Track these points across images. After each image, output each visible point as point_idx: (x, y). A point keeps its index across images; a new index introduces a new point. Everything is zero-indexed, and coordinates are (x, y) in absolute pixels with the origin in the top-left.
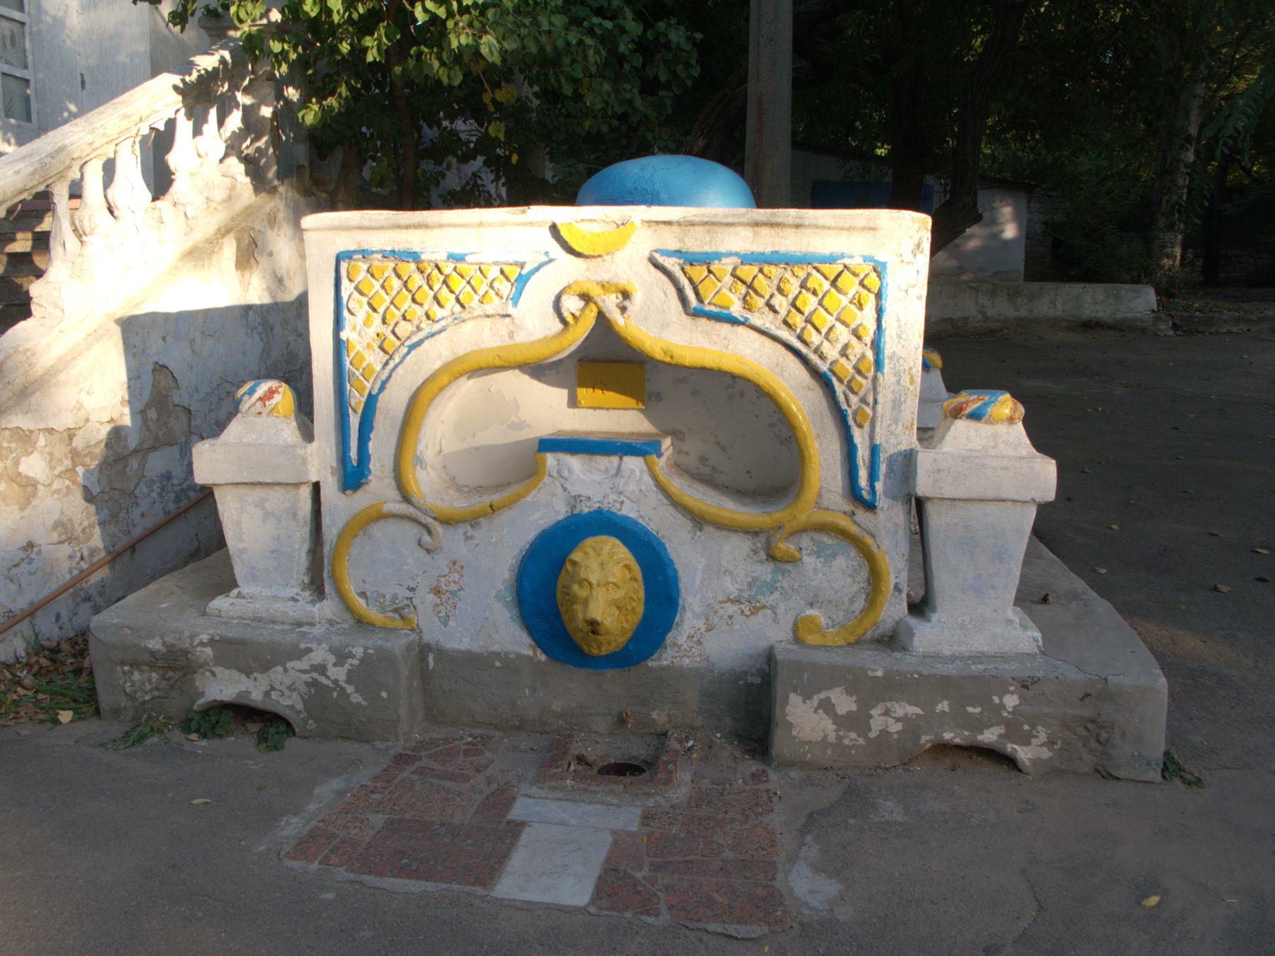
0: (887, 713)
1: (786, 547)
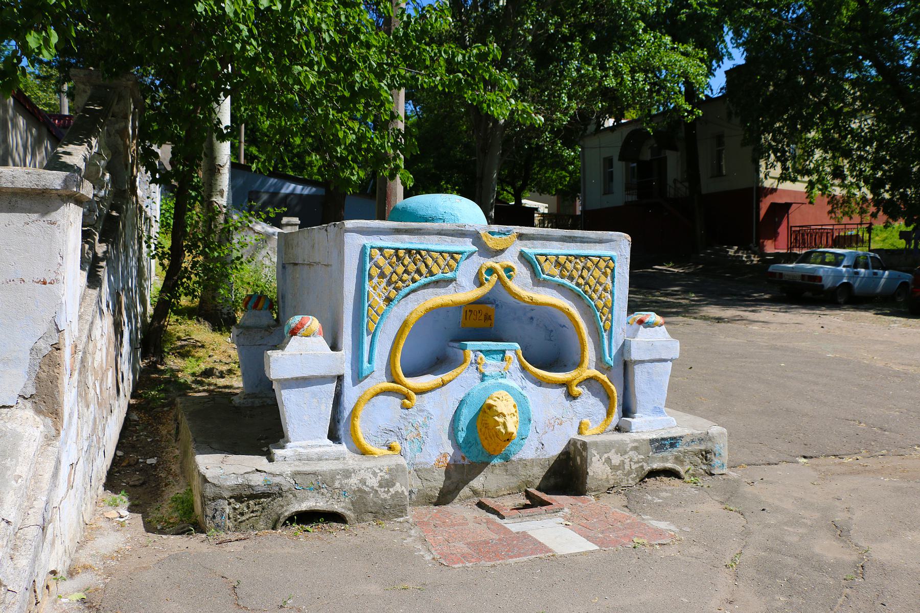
0: (631, 461)
1: (577, 390)
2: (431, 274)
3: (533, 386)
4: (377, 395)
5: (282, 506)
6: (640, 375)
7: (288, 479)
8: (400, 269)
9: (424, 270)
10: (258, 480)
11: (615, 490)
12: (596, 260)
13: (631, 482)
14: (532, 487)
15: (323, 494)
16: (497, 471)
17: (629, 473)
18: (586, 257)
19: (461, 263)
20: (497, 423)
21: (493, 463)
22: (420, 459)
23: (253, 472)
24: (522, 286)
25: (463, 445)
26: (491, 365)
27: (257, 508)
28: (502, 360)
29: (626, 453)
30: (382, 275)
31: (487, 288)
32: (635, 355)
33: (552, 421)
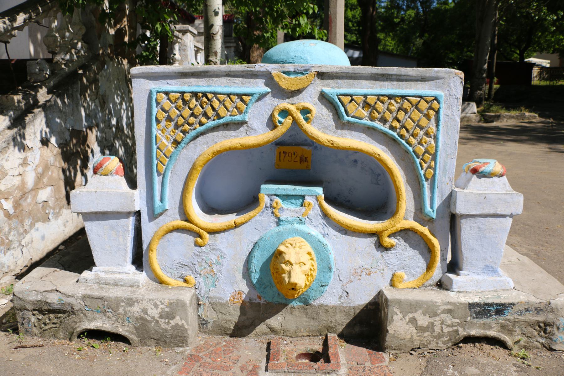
0: (442, 323)
1: (387, 241)
2: (219, 117)
3: (337, 233)
4: (171, 231)
5: (76, 323)
6: (467, 229)
7: (79, 300)
8: (187, 112)
9: (210, 113)
10: (54, 299)
11: (420, 351)
12: (414, 100)
13: (441, 345)
14: (333, 332)
15: (108, 317)
16: (297, 313)
17: (440, 336)
18: (403, 97)
19: (250, 105)
20: (283, 271)
21: (291, 304)
22: (214, 293)
23: (52, 291)
24: (322, 129)
25: (257, 286)
26: (289, 210)
27: (55, 321)
28: (301, 206)
29: (436, 315)
30: (169, 119)
31: (281, 130)
32: (460, 208)
33: (359, 271)
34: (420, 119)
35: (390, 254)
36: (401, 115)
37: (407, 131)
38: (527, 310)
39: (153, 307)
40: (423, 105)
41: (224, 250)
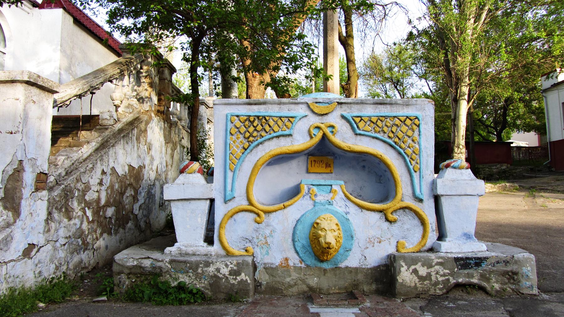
0: (437, 273)
4: (237, 212)
7: (167, 264)
8: (251, 129)
9: (267, 128)
12: (403, 119)
16: (328, 275)
19: (294, 124)
20: (320, 236)
23: (145, 258)
32: (440, 191)
33: (372, 240)
34: (407, 131)
35: (395, 227)
36: (394, 129)
37: (399, 139)
38: (498, 262)
39: (224, 267)
40: (408, 122)
41: (275, 226)
